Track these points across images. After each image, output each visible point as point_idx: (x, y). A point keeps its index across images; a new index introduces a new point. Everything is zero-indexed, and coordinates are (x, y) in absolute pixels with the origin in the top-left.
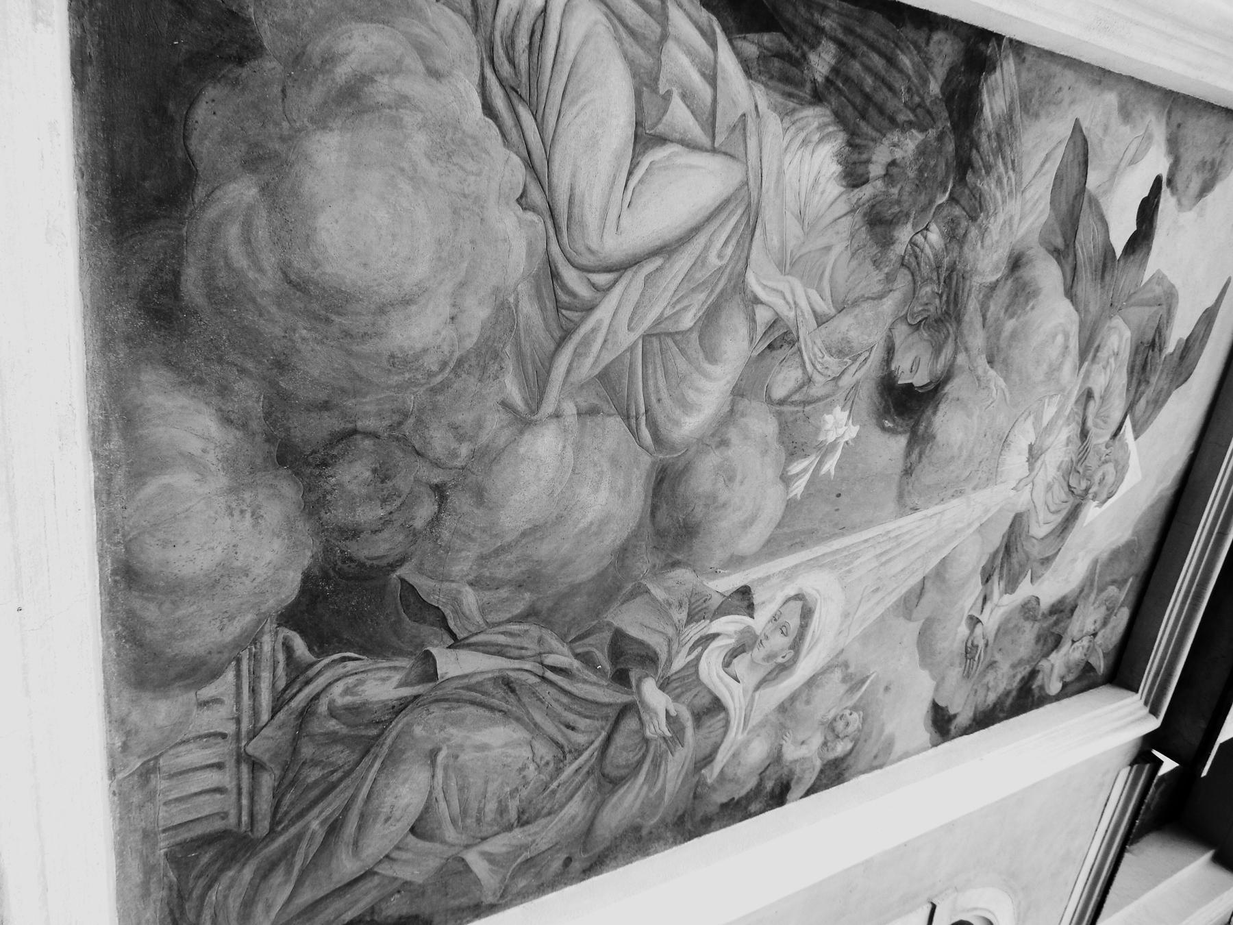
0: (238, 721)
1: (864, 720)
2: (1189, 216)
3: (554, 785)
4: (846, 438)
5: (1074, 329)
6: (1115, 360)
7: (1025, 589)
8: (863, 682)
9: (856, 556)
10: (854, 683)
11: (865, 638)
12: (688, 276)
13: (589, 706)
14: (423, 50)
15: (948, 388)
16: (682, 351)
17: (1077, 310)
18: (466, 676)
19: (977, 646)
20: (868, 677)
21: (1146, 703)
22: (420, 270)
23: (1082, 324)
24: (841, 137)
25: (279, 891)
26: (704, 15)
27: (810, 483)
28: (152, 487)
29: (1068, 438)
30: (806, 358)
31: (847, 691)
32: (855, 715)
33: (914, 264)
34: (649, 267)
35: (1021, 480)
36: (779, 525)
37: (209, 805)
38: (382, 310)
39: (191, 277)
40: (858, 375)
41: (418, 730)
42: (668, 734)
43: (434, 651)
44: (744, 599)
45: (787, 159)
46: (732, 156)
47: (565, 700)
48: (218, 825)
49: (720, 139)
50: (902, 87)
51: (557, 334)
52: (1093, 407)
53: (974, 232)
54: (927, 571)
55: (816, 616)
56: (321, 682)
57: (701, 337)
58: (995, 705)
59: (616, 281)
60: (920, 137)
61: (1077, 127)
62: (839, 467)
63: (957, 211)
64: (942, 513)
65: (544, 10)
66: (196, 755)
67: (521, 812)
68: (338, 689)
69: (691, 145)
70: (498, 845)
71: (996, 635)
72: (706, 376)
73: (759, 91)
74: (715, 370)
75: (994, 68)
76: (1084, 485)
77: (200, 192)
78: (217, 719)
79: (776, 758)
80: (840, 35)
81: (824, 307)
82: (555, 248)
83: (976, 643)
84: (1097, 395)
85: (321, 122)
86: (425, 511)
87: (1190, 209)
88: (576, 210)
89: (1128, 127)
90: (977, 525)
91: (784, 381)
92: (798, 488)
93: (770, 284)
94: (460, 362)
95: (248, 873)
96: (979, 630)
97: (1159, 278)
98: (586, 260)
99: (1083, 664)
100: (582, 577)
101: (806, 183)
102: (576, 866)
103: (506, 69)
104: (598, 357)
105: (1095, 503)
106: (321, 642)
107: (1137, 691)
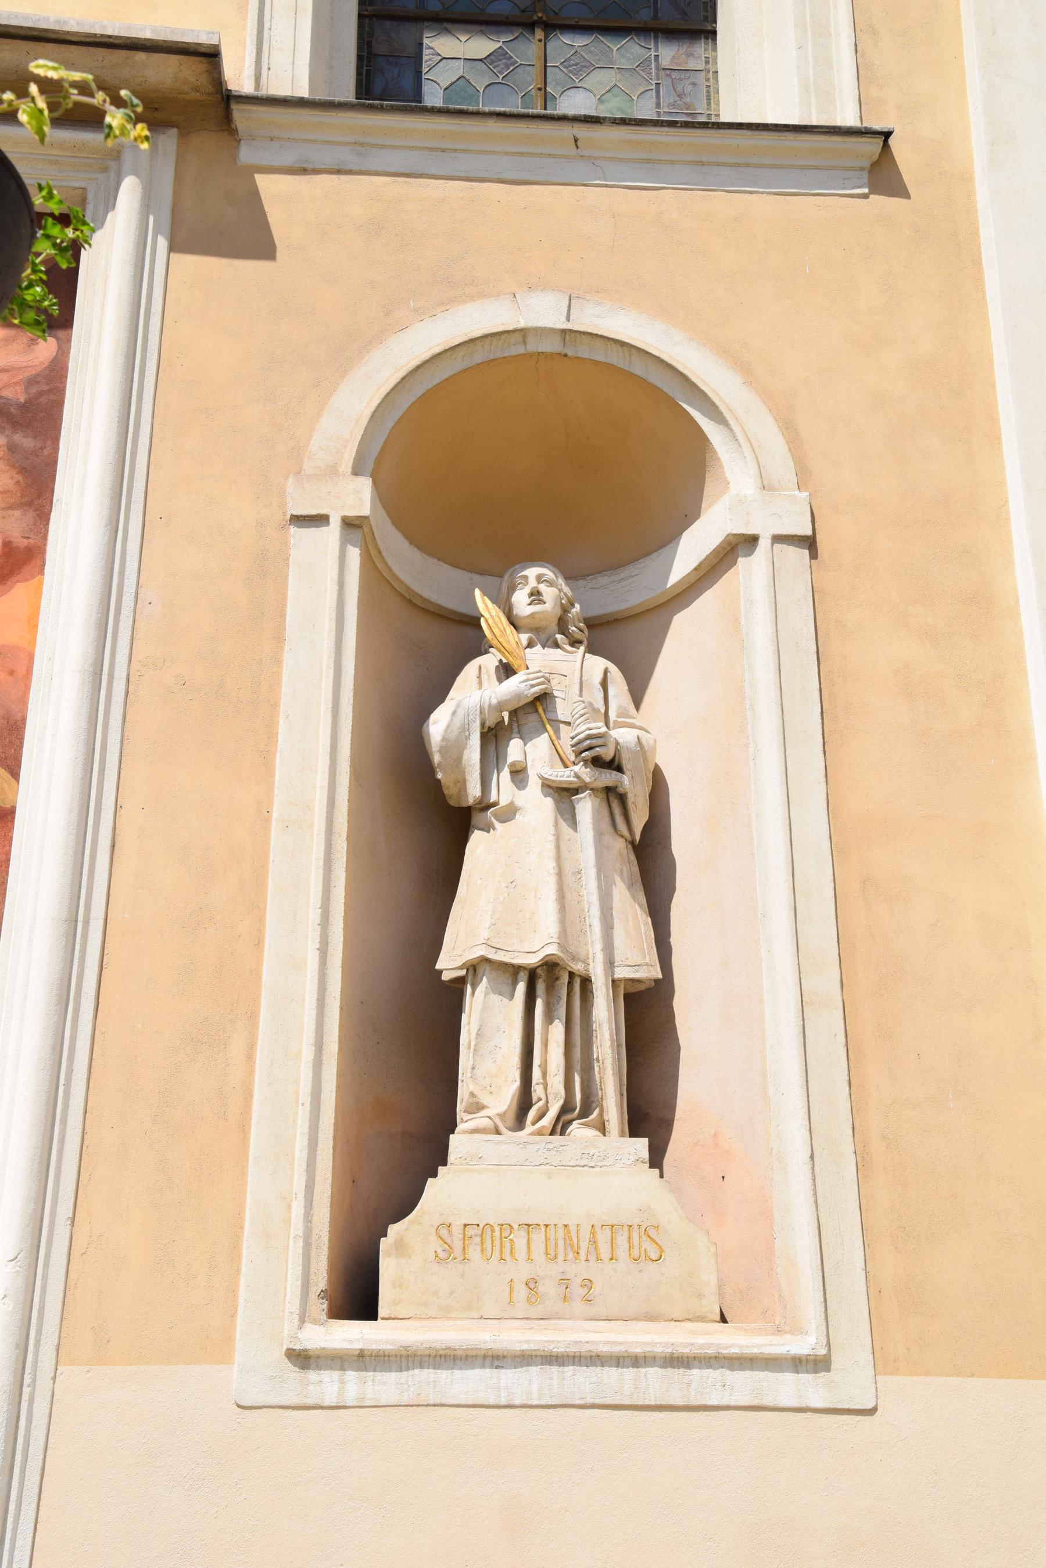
58: (23, 470)
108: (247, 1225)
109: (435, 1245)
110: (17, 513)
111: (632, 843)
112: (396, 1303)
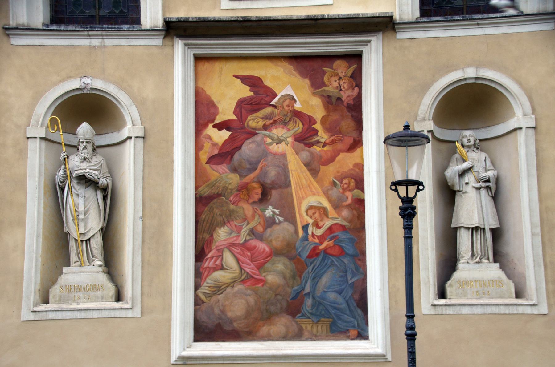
0: (310, 324)
1: (346, 178)
2: (220, 107)
3: (339, 266)
4: (272, 209)
5: (248, 141)
6: (255, 119)
7: (318, 126)
8: (334, 182)
9: (299, 196)
10: (334, 184)
11: (321, 186)
12: (242, 256)
13: (323, 259)
14: (216, 303)
15: (262, 182)
16: (254, 254)
17: (243, 144)
18: (310, 287)
19: (333, 139)
20: (333, 181)
21: (367, 45)
22: (243, 301)
23: (247, 139)
24: (217, 228)
25: (346, 317)
26: (204, 261)
27: (281, 216)
28: (272, 334)
29: (275, 128)
30: (255, 225)
31: (336, 187)
32: (344, 182)
33: (237, 202)
35: (286, 144)
36: (289, 222)
37: (324, 328)
38: (249, 306)
39: (245, 330)
40: (258, 209)
41: (319, 295)
42: (334, 240)
43: (304, 293)
44: (305, 228)
45: (222, 239)
46: (223, 251)
47: (320, 267)
48: (328, 327)
49: (221, 254)
50: (207, 218)
51: (252, 278)
52: (268, 122)
53: (230, 187)
54: (307, 170)
55: (312, 204)
56: (306, 312)
57: (252, 250)
58: (355, 121)
59: (243, 269)
60: (215, 209)
61: (207, 163)
62: (277, 209)
63: (226, 194)
64: (292, 170)
65: (209, 287)
66: (315, 330)
67: (343, 272)
68: (308, 309)
71: (331, 132)
72: (259, 247)
73: (213, 247)
74: (257, 245)
75: (201, 194)
76: (289, 114)
77: (235, 329)
78: (309, 327)
79: (349, 206)
80: (202, 234)
82: (239, 281)
83: (331, 141)
84: (264, 123)
85: (226, 315)
86: (279, 297)
87: (218, 108)
88: (234, 278)
89: (205, 145)
90: (296, 156)
91: (260, 229)
92: (281, 219)
93: (242, 237)
94: (256, 294)
95: (340, 322)
96: (327, 142)
97: (235, 113)
98: (240, 274)
99: (351, 79)
100: (295, 267)
101: (225, 234)
102: (361, 257)
103: (216, 292)
104: (255, 270)
105: (295, 105)
106: (299, 311)
107: (362, 51)
108: (421, 282)
109: (458, 285)
110: (355, 132)
111: (492, 197)
112: (451, 296)
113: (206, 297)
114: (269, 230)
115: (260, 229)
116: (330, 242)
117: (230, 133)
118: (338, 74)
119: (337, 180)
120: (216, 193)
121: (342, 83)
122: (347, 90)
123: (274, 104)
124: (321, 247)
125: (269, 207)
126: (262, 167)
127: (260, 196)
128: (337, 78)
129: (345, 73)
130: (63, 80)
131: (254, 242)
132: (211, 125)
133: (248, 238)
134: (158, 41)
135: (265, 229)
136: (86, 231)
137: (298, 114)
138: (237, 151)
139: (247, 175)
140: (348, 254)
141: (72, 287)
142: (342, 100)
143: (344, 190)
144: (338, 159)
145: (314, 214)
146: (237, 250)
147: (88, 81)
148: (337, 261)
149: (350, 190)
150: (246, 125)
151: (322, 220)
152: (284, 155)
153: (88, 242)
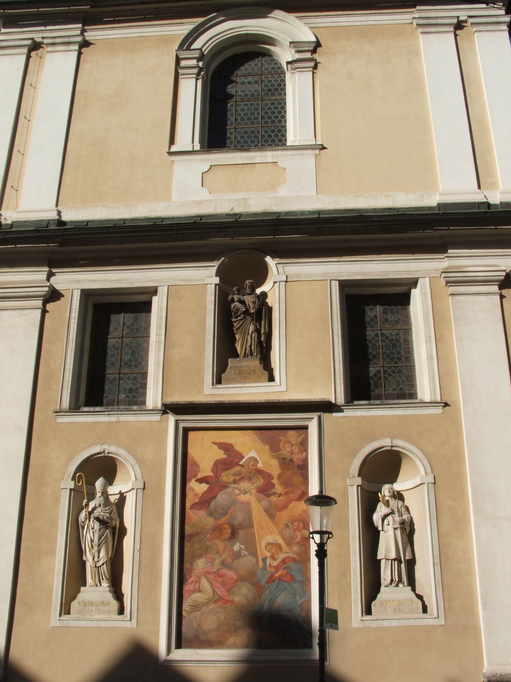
1: (296, 521)
2: (201, 466)
4: (239, 545)
7: (275, 481)
10: (287, 526)
13: (277, 586)
17: (218, 494)
19: (286, 491)
21: (311, 421)
23: (221, 490)
29: (243, 483)
34: (214, 587)
44: (264, 560)
45: (200, 568)
46: (200, 577)
52: (237, 478)
53: (207, 527)
55: (270, 542)
63: (204, 532)
64: (254, 515)
65: (189, 605)
69: (200, 584)
70: (298, 598)
73: (193, 574)
74: (227, 573)
79: (298, 543)
81: (218, 556)
82: (212, 601)
84: (234, 478)
90: (258, 504)
91: (229, 560)
92: (246, 553)
96: (282, 493)
97: (212, 471)
105: (258, 465)
107: (308, 425)
113: (187, 614)
114: (236, 561)
115: (229, 560)
116: (284, 571)
117: (207, 486)
118: (290, 442)
119: (289, 523)
120: (196, 532)
121: (293, 448)
122: (298, 453)
123: (242, 464)
124: (277, 575)
125: (236, 543)
126: (232, 512)
127: (230, 535)
128: (289, 445)
129: (296, 441)
130: (89, 446)
131: (224, 571)
132: (194, 480)
133: (220, 567)
134: (157, 417)
135: (233, 561)
136: (99, 560)
137: (260, 472)
138: (212, 501)
139: (220, 519)
140: (297, 581)
141: (87, 603)
142: (293, 461)
143: (295, 530)
144: (290, 506)
145: (271, 549)
146: (211, 577)
147: (105, 447)
148: (289, 586)
149: (299, 531)
150: (220, 480)
151: (277, 554)
152: (249, 504)
153: (100, 568)
